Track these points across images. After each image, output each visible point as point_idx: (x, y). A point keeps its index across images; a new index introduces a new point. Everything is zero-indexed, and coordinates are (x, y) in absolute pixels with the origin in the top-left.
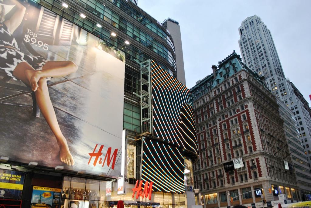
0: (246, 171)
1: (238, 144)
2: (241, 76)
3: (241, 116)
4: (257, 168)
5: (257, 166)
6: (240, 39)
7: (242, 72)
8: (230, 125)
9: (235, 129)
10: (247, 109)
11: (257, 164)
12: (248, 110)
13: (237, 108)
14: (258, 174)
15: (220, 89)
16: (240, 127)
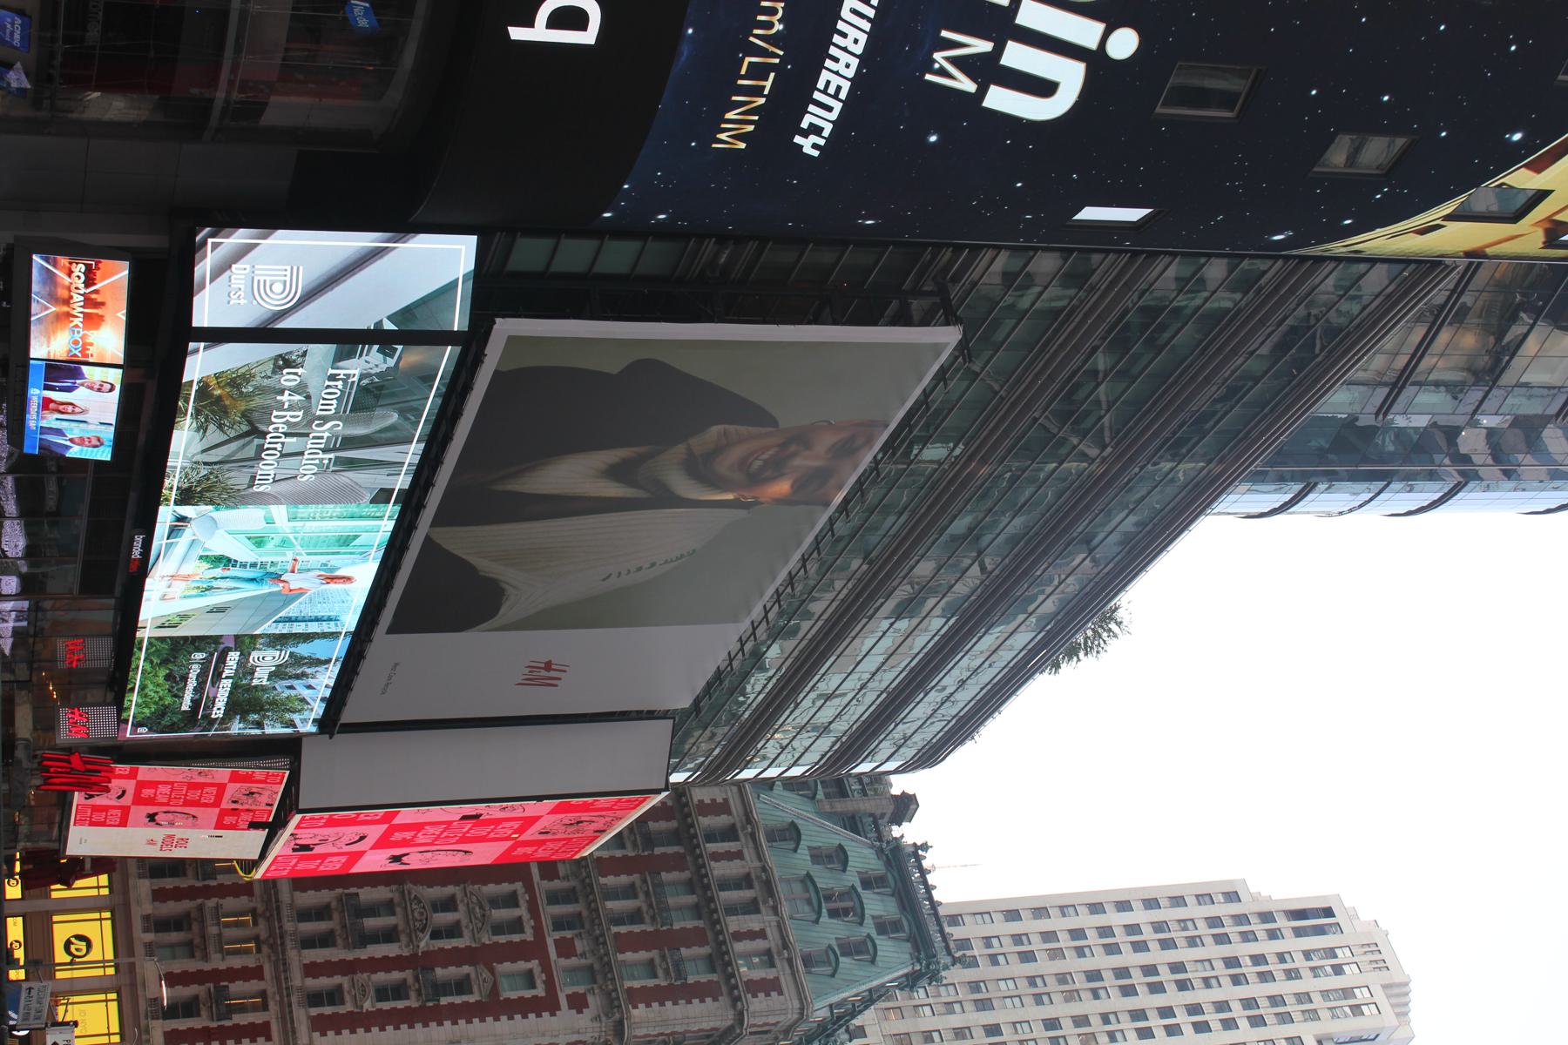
0: (206, 958)
1: (371, 923)
2: (774, 994)
3: (528, 965)
4: (214, 1025)
5: (227, 1023)
6: (1255, 898)
7: (796, 1004)
8: (491, 889)
9: (459, 915)
10: (563, 1002)
11: (237, 1026)
12: (554, 1008)
13: (579, 946)
14: (182, 1024)
15: (731, 846)
16: (468, 948)
